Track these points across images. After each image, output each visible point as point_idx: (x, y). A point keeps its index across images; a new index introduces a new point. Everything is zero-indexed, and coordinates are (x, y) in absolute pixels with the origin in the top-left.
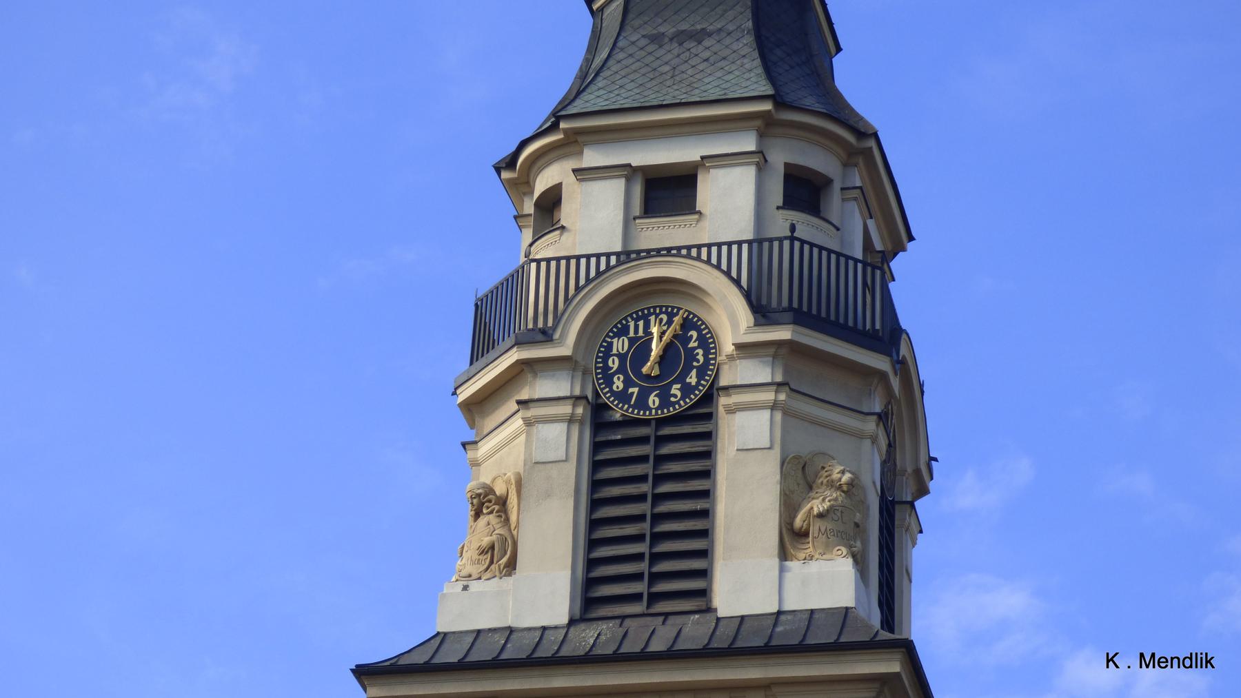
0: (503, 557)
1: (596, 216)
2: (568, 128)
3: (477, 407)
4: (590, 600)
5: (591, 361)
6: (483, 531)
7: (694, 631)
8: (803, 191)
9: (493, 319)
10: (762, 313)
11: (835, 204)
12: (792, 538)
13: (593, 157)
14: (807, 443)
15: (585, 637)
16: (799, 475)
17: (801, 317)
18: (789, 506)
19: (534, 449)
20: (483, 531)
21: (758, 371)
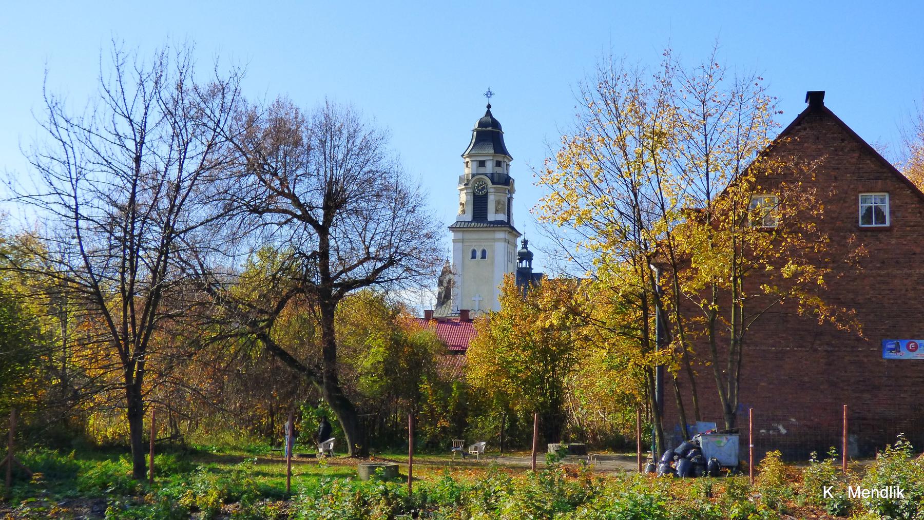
8: (498, 164)
10: (493, 183)
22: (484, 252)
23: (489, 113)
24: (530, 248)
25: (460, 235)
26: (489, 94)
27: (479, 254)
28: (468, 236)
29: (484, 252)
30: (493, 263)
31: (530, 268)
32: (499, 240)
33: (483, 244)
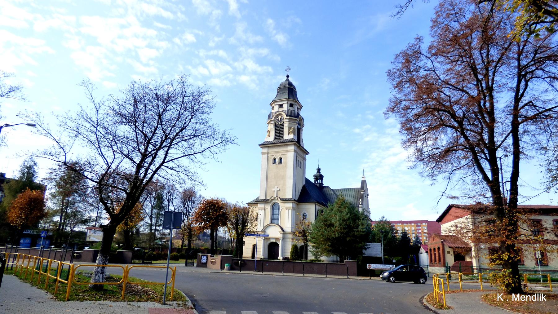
0: (269, 136)
1: (276, 108)
2: (274, 102)
3: (268, 124)
4: (275, 139)
5: (275, 120)
6: (268, 134)
7: (282, 141)
8: (291, 105)
9: (269, 117)
11: (294, 106)
12: (289, 133)
13: (276, 104)
14: (290, 125)
15: (275, 141)
16: (290, 128)
17: (290, 116)
18: (289, 131)
19: (272, 127)
20: (268, 134)
21: (287, 120)
22: (281, 159)
23: (288, 80)
24: (322, 172)
25: (265, 150)
26: (288, 69)
27: (277, 160)
28: (271, 150)
29: (281, 159)
30: (286, 166)
31: (322, 184)
32: (290, 151)
33: (280, 154)
